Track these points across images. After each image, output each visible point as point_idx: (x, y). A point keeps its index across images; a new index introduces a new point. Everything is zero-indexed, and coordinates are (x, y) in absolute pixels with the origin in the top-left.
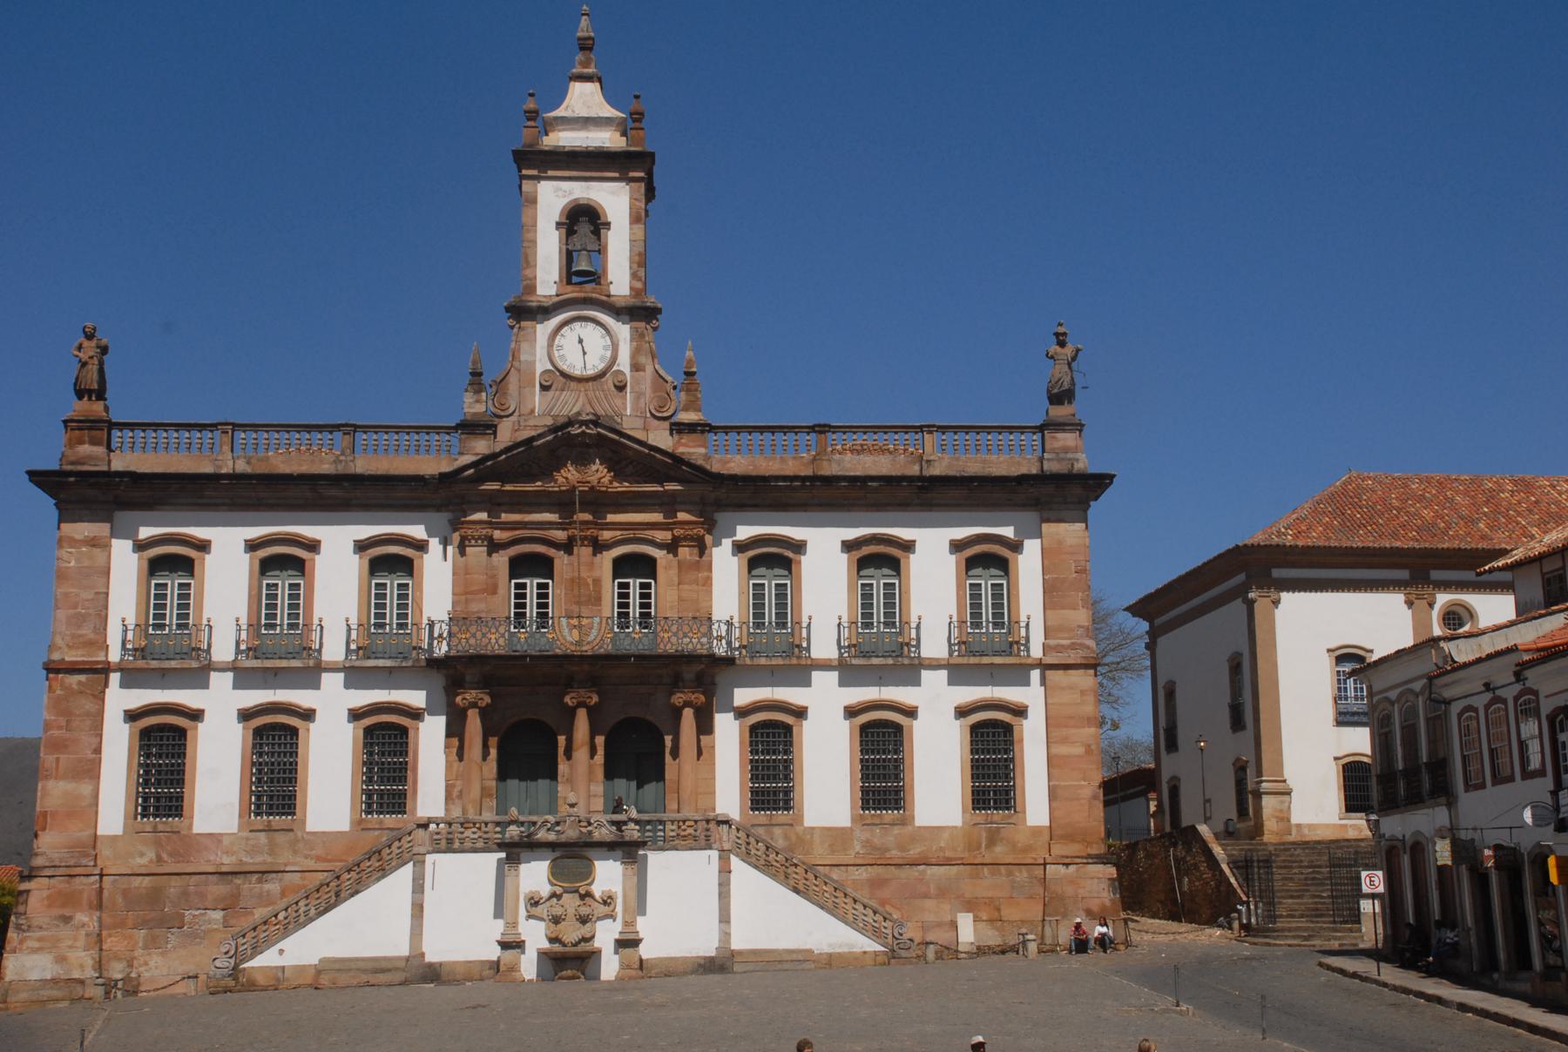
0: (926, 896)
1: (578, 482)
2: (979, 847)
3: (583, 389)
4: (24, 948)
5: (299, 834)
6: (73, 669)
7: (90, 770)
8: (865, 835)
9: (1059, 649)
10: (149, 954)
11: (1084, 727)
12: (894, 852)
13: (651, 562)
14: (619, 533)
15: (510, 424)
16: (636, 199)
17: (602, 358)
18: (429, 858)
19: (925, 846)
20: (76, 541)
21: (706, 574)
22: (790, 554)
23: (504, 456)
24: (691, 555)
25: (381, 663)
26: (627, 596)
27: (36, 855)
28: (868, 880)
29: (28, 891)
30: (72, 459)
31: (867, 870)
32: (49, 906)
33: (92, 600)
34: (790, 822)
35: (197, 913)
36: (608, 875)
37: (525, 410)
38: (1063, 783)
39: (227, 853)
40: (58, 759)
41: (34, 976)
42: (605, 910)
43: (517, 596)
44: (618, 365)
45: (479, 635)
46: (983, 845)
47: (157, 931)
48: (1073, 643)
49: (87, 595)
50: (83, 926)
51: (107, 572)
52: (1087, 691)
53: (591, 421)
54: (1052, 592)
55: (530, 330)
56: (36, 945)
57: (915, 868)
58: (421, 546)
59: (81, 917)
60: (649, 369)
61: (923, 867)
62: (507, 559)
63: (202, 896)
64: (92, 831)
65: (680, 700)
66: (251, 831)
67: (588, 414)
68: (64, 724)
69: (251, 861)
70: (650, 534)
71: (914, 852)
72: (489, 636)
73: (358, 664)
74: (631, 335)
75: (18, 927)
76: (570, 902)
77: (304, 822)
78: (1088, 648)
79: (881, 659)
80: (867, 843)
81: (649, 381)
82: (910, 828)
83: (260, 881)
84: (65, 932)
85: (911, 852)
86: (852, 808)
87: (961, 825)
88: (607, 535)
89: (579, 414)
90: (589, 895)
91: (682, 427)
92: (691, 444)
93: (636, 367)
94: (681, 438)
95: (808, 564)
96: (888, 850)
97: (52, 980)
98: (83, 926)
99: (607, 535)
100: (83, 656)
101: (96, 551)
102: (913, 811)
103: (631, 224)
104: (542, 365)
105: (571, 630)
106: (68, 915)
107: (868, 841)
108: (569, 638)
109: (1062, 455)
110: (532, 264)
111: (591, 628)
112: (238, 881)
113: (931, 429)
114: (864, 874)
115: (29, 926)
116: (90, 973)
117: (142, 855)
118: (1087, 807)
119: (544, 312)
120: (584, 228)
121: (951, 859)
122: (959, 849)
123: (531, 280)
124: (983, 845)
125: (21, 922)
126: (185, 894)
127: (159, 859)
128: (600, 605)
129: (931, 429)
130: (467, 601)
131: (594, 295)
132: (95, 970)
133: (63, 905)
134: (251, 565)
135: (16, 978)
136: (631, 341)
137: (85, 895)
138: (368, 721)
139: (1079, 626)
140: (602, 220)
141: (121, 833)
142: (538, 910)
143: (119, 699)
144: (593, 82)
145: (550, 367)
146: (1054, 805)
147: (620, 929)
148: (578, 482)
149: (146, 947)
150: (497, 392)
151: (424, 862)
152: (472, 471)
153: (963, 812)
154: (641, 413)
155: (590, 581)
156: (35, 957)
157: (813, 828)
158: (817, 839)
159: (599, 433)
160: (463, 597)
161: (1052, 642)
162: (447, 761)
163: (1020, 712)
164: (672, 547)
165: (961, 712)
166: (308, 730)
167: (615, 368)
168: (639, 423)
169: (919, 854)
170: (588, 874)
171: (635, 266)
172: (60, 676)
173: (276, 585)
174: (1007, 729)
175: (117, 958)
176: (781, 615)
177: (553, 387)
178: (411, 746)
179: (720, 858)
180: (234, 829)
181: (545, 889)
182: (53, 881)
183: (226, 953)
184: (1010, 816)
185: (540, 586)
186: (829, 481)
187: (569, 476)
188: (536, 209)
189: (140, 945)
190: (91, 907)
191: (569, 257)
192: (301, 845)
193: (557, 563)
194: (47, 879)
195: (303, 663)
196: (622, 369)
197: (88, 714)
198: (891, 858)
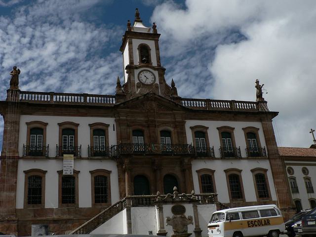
7: (13, 188)
17: (152, 81)
18: (132, 209)
22: (204, 131)
42: (189, 221)
45: (129, 149)
51: (18, 131)
58: (108, 126)
62: (131, 130)
77: (78, 205)
83: (66, 223)
90: (185, 217)
99: (157, 124)
104: (137, 81)
105: (154, 147)
117: (29, 215)
119: (137, 68)
127: (35, 216)
134: (59, 131)
136: (159, 77)
142: (170, 222)
152: (122, 105)
153: (257, 197)
159: (155, 97)
163: (266, 170)
164: (175, 127)
170: (183, 210)
173: (66, 137)
180: (57, 207)
181: (171, 215)
190: (15, 231)
193: (145, 132)
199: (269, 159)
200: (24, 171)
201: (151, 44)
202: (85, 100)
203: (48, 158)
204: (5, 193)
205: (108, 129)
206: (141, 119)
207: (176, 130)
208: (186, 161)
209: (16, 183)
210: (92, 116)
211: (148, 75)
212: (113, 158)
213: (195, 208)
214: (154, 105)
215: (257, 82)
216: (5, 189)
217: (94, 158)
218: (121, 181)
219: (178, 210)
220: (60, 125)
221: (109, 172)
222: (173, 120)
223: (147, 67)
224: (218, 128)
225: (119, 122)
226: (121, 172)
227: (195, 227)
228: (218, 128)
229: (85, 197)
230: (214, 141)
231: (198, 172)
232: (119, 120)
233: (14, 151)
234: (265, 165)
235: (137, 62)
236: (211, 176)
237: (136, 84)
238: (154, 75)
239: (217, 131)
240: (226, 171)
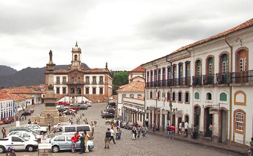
18: (66, 97)
36: (75, 98)
76: (73, 100)
104: (73, 65)
164: (81, 77)
170: (74, 98)
174: (102, 89)
186: (91, 73)
201: (78, 54)
212: (67, 84)
213: (77, 97)
219: (73, 98)
220: (56, 77)
221: (66, 87)
226: (68, 87)
229: (61, 92)
230: (91, 80)
234: (103, 86)
235: (74, 60)
238: (77, 63)
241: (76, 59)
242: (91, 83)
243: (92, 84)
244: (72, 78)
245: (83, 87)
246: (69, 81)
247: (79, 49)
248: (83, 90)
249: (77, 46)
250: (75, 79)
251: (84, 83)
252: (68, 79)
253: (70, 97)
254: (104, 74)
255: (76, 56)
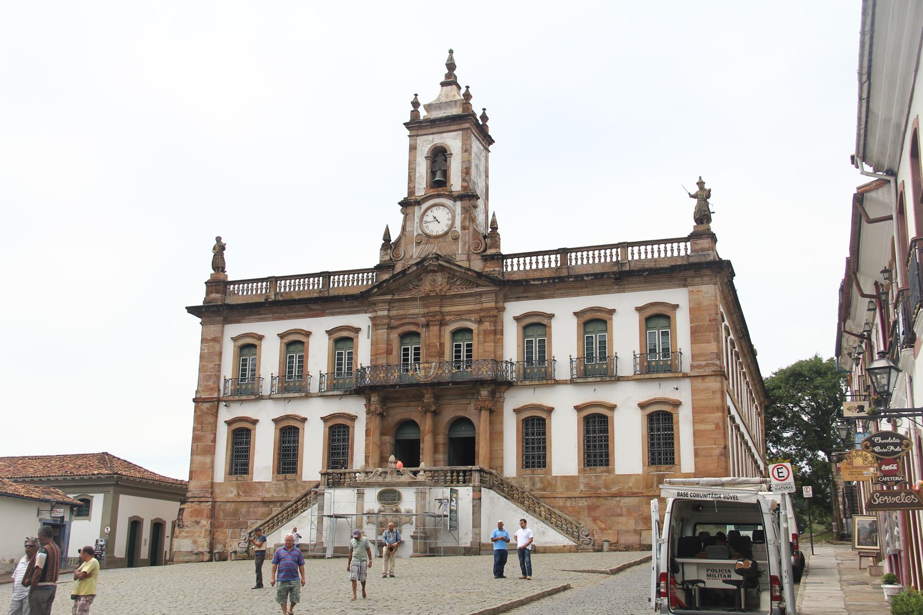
0: (621, 515)
1: (430, 291)
2: (652, 486)
3: (436, 242)
4: (181, 535)
5: (299, 482)
6: (205, 401)
8: (585, 481)
9: (698, 367)
10: (232, 541)
11: (714, 413)
12: (603, 490)
13: (470, 331)
14: (453, 317)
15: (401, 264)
16: (465, 140)
19: (621, 486)
20: (208, 340)
21: (498, 337)
22: (545, 322)
23: (392, 281)
24: (490, 326)
25: (335, 393)
26: (460, 351)
27: (188, 491)
28: (587, 506)
29: (183, 509)
30: (207, 301)
31: (586, 500)
32: (191, 516)
33: (213, 368)
34: (544, 473)
35: (253, 521)
37: (408, 256)
38: (701, 447)
39: (267, 491)
40: (197, 445)
41: (184, 549)
43: (404, 355)
44: (455, 228)
46: (655, 486)
47: (237, 530)
48: (707, 363)
49: (211, 365)
50: (204, 526)
51: (220, 354)
52: (716, 391)
53: (435, 258)
54: (695, 333)
55: (411, 215)
56: (186, 535)
57: (614, 499)
58: (357, 330)
59: (204, 522)
60: (471, 228)
61: (618, 499)
62: (397, 335)
63: (255, 513)
64: (207, 482)
65: (478, 406)
66: (277, 481)
67: (433, 254)
68: (200, 428)
69: (278, 496)
70: (467, 317)
71: (614, 489)
72: (381, 376)
73: (324, 394)
74: (461, 211)
75: (179, 525)
78: (717, 365)
79: (593, 378)
80: (587, 485)
81: (471, 235)
82: (612, 476)
84: (197, 528)
85: (613, 490)
86: (579, 465)
87: (642, 473)
88: (447, 318)
89: (429, 255)
90: (397, 511)
91: (487, 257)
92: (492, 266)
93: (464, 228)
94: (487, 264)
95: (556, 327)
96: (599, 489)
97: (191, 552)
98: (204, 526)
99: (447, 318)
100: (208, 395)
101: (217, 346)
102: (614, 466)
103: (462, 153)
106: (198, 520)
107: (587, 484)
108: (419, 375)
109: (700, 253)
110: (413, 180)
111: (431, 368)
112: (271, 506)
113: (624, 245)
114: (585, 503)
115: (183, 526)
116: (206, 549)
117: (232, 492)
118: (717, 461)
119: (418, 203)
120: (440, 158)
121: (635, 493)
122: (641, 488)
123: (412, 188)
124: (655, 486)
125: (181, 523)
126: (248, 512)
127: (239, 495)
128: (444, 357)
129: (624, 245)
130: (377, 359)
131: (442, 192)
132: (208, 548)
133: (197, 516)
135: (177, 550)
137: (206, 511)
138: (330, 424)
139: (711, 353)
140: (448, 153)
141: (223, 481)
143: (225, 414)
144: (451, 85)
145: (421, 233)
146: (698, 459)
147: (414, 530)
148: (430, 291)
149: (231, 538)
150: (395, 248)
151: (324, 494)
152: (376, 290)
153: (643, 466)
154: (466, 252)
155: (438, 344)
156: (184, 540)
157: (557, 477)
158: (559, 482)
159: (440, 265)
160: (375, 357)
161: (695, 363)
162: (366, 444)
163: (677, 404)
164: (480, 322)
165: (642, 406)
166: (304, 429)
167: (453, 229)
168: (465, 257)
169: (617, 490)
171: (464, 175)
172: (200, 404)
175: (220, 543)
176: (542, 359)
177: (422, 243)
178: (350, 436)
179: (473, 491)
182: (193, 504)
183: (244, 540)
184: (671, 468)
185: (416, 349)
187: (427, 289)
188: (416, 152)
189: (229, 536)
191: (433, 173)
192: (299, 488)
193: (422, 335)
194: (190, 503)
195: (300, 395)
196: (456, 229)
197: (210, 423)
198: (600, 493)
199: (685, 376)
200: (225, 422)
201: (453, 141)
202: (326, 284)
203: (260, 398)
204: (199, 457)
205: (358, 337)
206: (416, 310)
207: (482, 328)
208: (484, 393)
209: (214, 441)
210: (333, 314)
211: (442, 214)
212: (359, 391)
214: (440, 279)
215: (701, 184)
216: (198, 451)
217: (330, 393)
218: (367, 434)
220: (281, 336)
221: (353, 418)
222: (478, 307)
223: (439, 196)
224: (575, 314)
225: (376, 323)
227: (414, 530)
228: (575, 314)
231: (517, 411)
232: (375, 317)
233: (212, 389)
236: (544, 420)
237: (415, 236)
239: (574, 320)
240: (578, 408)
241: (439, 182)
242: (563, 370)
243: (572, 382)
244: (404, 336)
245: (495, 413)
246: (382, 361)
247: (467, 96)
248: (496, 436)
249: (450, 81)
250: (428, 346)
251: (511, 376)
252: (374, 344)
253: (361, 495)
254: (685, 286)
255: (439, 155)
